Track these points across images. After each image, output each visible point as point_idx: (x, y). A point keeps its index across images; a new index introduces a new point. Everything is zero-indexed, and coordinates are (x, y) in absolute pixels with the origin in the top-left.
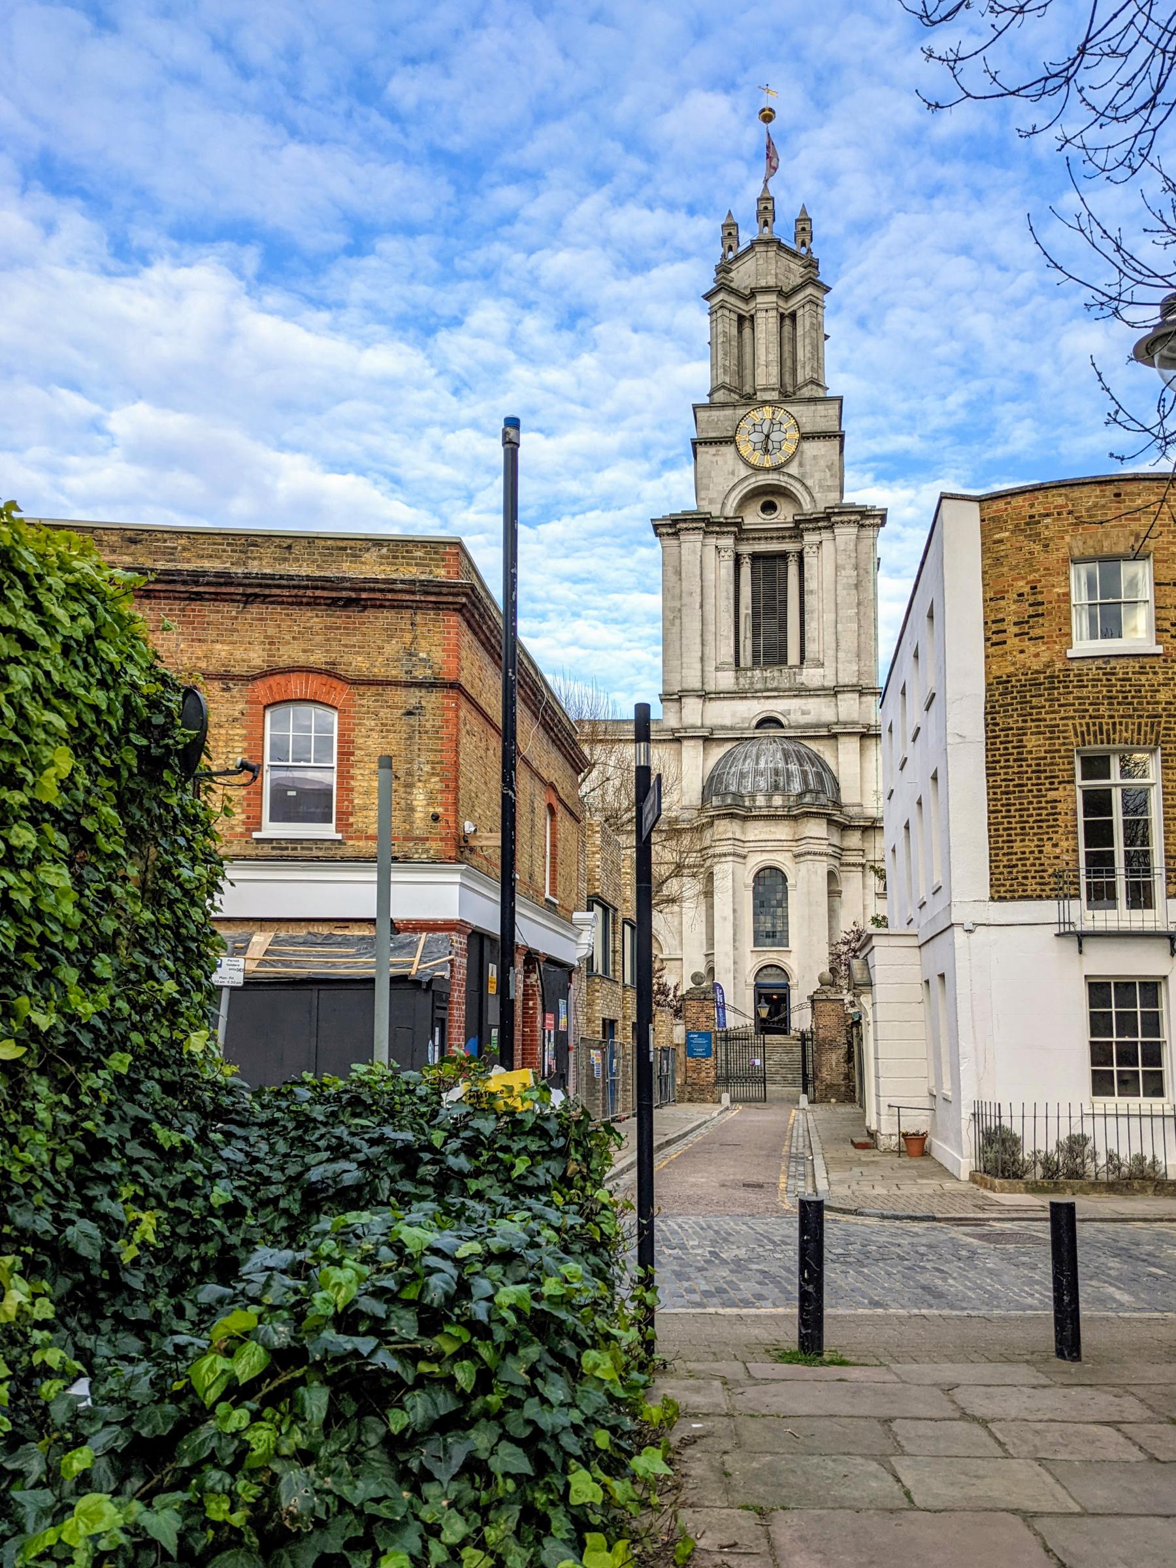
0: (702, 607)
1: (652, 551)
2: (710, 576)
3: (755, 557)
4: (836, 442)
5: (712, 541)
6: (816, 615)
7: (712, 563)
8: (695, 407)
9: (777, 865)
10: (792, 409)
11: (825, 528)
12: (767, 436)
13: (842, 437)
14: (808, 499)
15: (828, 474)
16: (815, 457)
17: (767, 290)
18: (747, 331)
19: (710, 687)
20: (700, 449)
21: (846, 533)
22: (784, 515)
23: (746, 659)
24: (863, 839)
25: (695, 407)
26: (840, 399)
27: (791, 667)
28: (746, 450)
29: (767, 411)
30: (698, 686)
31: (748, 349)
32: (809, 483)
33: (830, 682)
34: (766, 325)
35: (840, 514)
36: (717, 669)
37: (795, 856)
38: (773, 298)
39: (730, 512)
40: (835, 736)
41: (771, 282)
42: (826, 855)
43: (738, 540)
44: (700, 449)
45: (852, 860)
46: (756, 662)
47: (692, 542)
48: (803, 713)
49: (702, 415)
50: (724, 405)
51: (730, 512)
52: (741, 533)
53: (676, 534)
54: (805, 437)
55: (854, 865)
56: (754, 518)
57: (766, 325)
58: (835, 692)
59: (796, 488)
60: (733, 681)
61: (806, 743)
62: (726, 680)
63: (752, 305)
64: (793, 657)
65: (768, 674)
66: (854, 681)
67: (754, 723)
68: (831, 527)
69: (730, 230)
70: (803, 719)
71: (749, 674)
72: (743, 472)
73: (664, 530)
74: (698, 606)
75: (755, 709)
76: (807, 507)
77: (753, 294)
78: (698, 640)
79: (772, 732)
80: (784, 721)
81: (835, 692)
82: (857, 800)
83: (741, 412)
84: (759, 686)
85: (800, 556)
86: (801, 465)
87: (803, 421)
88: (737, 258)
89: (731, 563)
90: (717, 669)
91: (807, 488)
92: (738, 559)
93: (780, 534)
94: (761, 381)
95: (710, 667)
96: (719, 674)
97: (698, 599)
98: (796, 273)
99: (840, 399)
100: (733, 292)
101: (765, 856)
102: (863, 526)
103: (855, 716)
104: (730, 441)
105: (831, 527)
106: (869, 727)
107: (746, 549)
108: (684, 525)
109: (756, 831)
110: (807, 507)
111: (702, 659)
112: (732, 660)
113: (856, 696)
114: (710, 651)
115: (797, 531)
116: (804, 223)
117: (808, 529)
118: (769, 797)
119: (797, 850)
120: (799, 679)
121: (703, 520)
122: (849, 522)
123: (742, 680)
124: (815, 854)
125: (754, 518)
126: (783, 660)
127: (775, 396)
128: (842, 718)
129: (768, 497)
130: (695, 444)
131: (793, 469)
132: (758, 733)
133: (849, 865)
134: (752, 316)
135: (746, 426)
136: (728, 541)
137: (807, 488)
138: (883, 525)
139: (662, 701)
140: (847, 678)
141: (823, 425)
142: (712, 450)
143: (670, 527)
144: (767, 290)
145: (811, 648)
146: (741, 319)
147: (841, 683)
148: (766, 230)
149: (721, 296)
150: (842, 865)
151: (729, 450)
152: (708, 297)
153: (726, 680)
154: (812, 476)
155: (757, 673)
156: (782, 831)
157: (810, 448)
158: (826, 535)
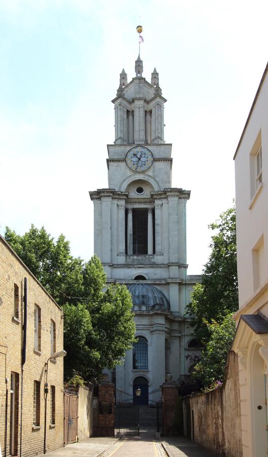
0: (111, 229)
1: (90, 204)
2: (115, 217)
4: (169, 163)
5: (116, 202)
7: (116, 211)
9: (143, 335)
11: (164, 198)
12: (139, 159)
13: (171, 160)
14: (157, 186)
15: (165, 176)
17: (140, 99)
18: (131, 117)
19: (115, 263)
20: (110, 163)
21: (173, 200)
22: (146, 194)
23: (130, 251)
24: (180, 326)
27: (149, 255)
28: (130, 165)
29: (139, 149)
30: (109, 261)
31: (131, 125)
33: (166, 262)
34: (139, 115)
35: (170, 191)
36: (118, 255)
37: (152, 332)
38: (142, 102)
39: (123, 189)
40: (168, 284)
41: (141, 96)
42: (164, 331)
43: (127, 202)
44: (110, 163)
45: (175, 335)
46: (134, 253)
47: (107, 201)
48: (155, 274)
49: (111, 149)
50: (121, 145)
51: (123, 189)
52: (128, 200)
53: (99, 198)
54: (155, 160)
55: (176, 337)
56: (134, 194)
57: (139, 115)
58: (168, 266)
59: (152, 181)
60: (124, 260)
61: (155, 286)
62: (122, 260)
63: (133, 105)
64: (150, 251)
65: (139, 258)
66: (177, 261)
67: (134, 278)
68: (166, 198)
69: (123, 76)
70: (155, 277)
71: (131, 257)
72: (129, 173)
73: (95, 197)
74: (109, 228)
75: (136, 272)
76: (156, 189)
77: (133, 101)
78: (110, 243)
79: (141, 282)
80: (146, 277)
81: (168, 266)
82: (177, 310)
86: (154, 172)
87: (155, 153)
88: (126, 87)
89: (124, 212)
90: (118, 255)
91: (156, 181)
94: (136, 137)
95: (115, 254)
96: (118, 257)
97: (110, 226)
98: (151, 93)
100: (125, 99)
102: (180, 198)
103: (177, 276)
104: (124, 160)
105: (166, 198)
106: (183, 280)
108: (103, 194)
110: (156, 189)
112: (124, 251)
115: (152, 199)
116: (155, 75)
117: (157, 199)
118: (140, 307)
119: (152, 329)
120: (153, 260)
121: (112, 192)
122: (174, 196)
123: (128, 260)
124: (160, 331)
126: (145, 252)
127: (143, 143)
128: (172, 276)
129: (139, 186)
130: (108, 161)
131: (150, 173)
132: (135, 282)
133: (173, 336)
134: (133, 111)
135: (131, 154)
136: (122, 203)
137: (156, 181)
138: (189, 198)
140: (173, 260)
141: (163, 156)
143: (97, 195)
144: (140, 99)
145: (158, 248)
146: (128, 111)
147: (171, 261)
148: (139, 75)
149: (119, 100)
151: (123, 164)
152: (113, 101)
153: (122, 260)
155: (135, 257)
157: (157, 164)
158: (164, 201)
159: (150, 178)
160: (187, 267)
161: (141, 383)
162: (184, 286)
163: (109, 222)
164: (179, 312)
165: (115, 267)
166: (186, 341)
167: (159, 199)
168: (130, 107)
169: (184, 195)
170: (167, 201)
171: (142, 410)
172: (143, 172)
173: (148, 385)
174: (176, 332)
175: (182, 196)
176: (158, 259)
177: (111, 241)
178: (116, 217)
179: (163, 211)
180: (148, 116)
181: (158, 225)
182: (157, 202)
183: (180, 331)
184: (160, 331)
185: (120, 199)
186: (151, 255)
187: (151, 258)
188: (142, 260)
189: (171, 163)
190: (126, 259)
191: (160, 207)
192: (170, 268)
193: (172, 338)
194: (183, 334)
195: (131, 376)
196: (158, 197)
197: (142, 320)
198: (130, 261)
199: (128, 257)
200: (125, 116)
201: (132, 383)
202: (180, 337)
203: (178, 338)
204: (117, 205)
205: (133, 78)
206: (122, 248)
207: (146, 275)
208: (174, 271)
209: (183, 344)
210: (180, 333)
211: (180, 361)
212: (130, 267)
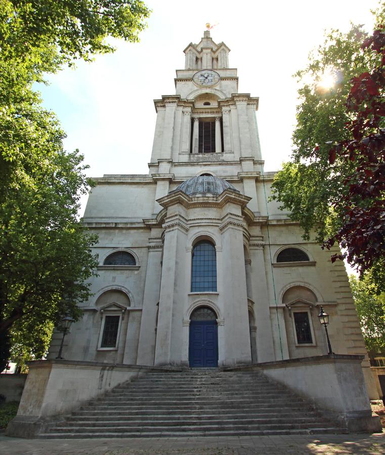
2: (179, 120)
3: (201, 121)
4: (235, 81)
5: (181, 109)
6: (229, 135)
8: (177, 71)
10: (218, 72)
12: (207, 78)
13: (237, 79)
16: (227, 85)
17: (207, 48)
20: (178, 83)
21: (242, 104)
22: (214, 104)
25: (177, 71)
26: (236, 69)
30: (168, 157)
32: (225, 92)
44: (178, 83)
45: (256, 242)
46: (200, 151)
52: (194, 109)
55: (257, 245)
56: (200, 105)
71: (196, 156)
73: (159, 105)
75: (199, 170)
78: (171, 140)
82: (257, 210)
83: (195, 72)
84: (201, 161)
85: (221, 120)
86: (220, 87)
92: (193, 120)
93: (212, 111)
95: (176, 153)
97: (172, 125)
99: (236, 69)
101: (201, 229)
104: (191, 79)
107: (196, 116)
109: (196, 213)
111: (172, 148)
113: (252, 163)
114: (177, 147)
117: (224, 106)
120: (221, 158)
123: (192, 158)
125: (200, 105)
126: (214, 150)
129: (206, 98)
130: (176, 80)
133: (254, 245)
134: (201, 59)
136: (189, 109)
139: (150, 166)
142: (183, 83)
145: (226, 147)
146: (197, 59)
150: (250, 245)
151: (190, 83)
153: (185, 158)
154: (225, 90)
155: (201, 156)
156: (212, 213)
157: (224, 83)
158: (232, 107)
159: (217, 92)
160: (264, 163)
161: (204, 326)
162: (262, 184)
163: (172, 122)
164: (259, 212)
165: (175, 166)
166: (273, 252)
167: (227, 106)
168: (199, 56)
169: (252, 101)
170: (235, 107)
171: (203, 376)
172: (209, 87)
173: (216, 323)
174: (258, 238)
175: (251, 103)
176: (227, 157)
177: (173, 139)
178: (180, 120)
179: (231, 117)
180: (215, 62)
181: (227, 126)
182: (224, 109)
183: (263, 237)
184: (234, 224)
185: (186, 107)
186: (219, 153)
187: (219, 156)
188: (209, 158)
189: (237, 82)
190: (190, 157)
191: (227, 112)
192: (243, 163)
193: (252, 248)
194: (267, 243)
195: (187, 306)
196: (226, 104)
197: (206, 213)
198: (194, 159)
199: (192, 156)
200: (195, 59)
201: (187, 319)
202: (263, 246)
203: (262, 248)
204: (183, 112)
205: (202, 38)
206: (186, 147)
207: (214, 173)
208: (248, 166)
209: (268, 257)
210: (262, 240)
211: (267, 284)
212: (193, 165)
